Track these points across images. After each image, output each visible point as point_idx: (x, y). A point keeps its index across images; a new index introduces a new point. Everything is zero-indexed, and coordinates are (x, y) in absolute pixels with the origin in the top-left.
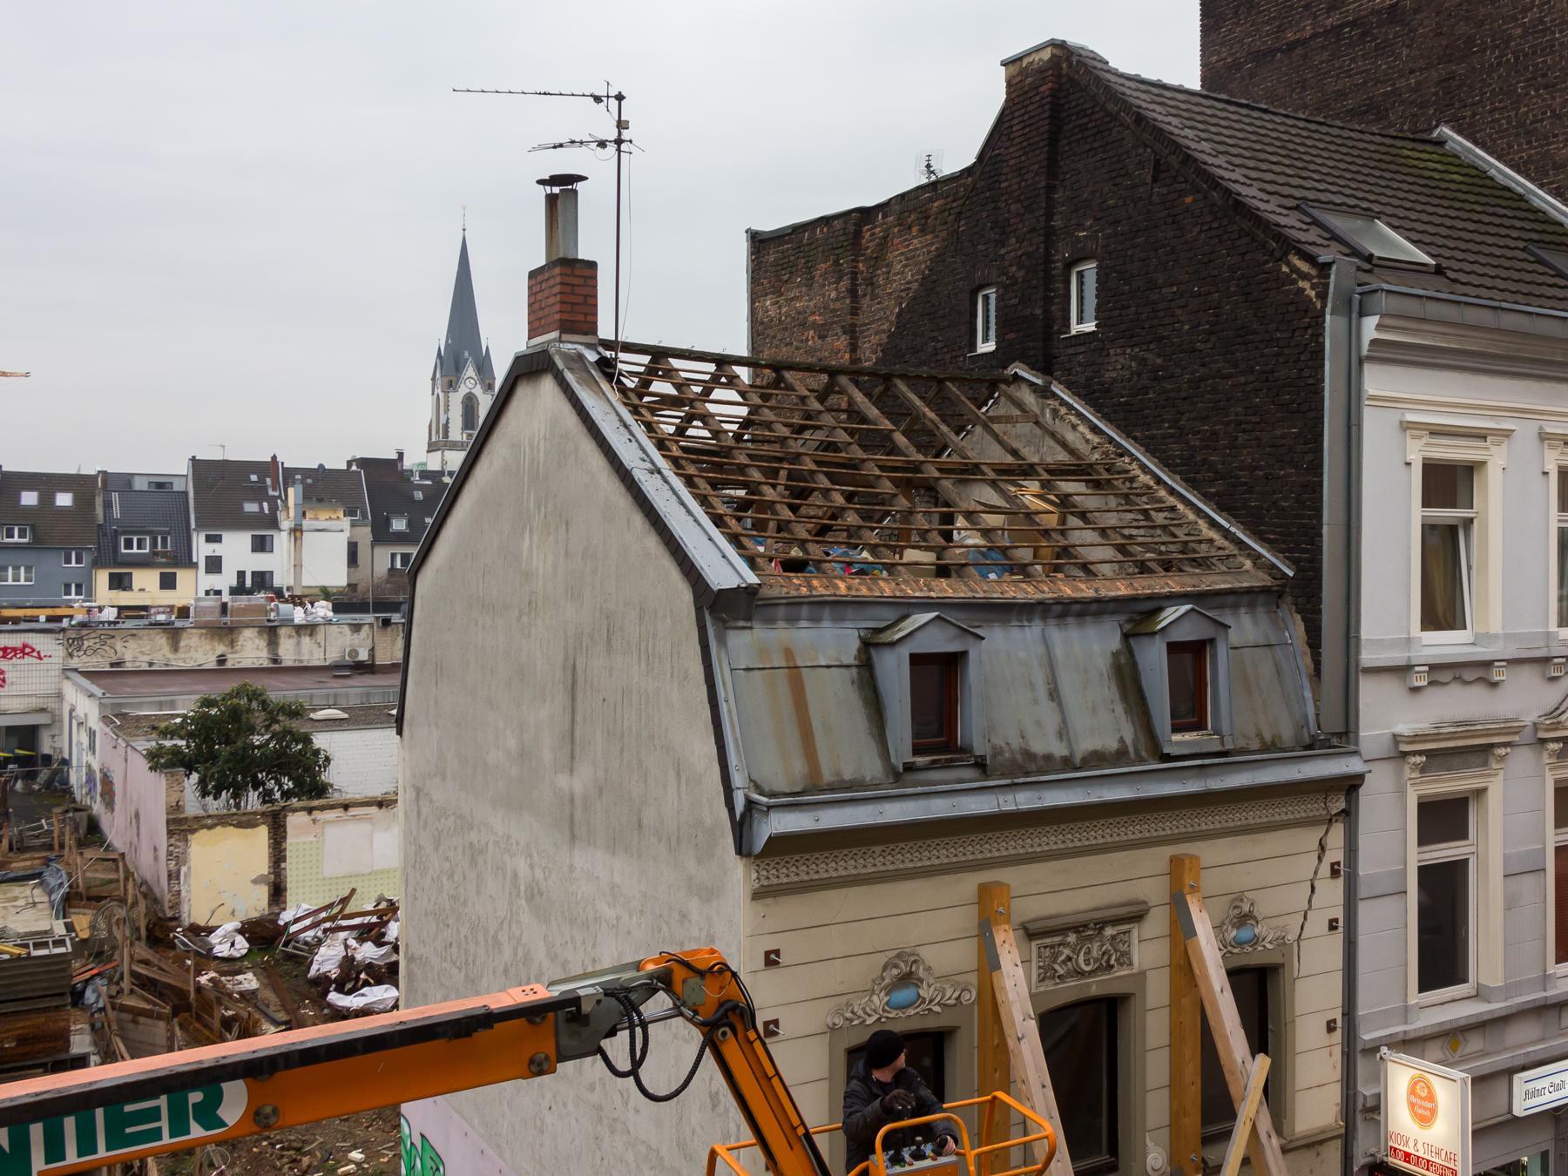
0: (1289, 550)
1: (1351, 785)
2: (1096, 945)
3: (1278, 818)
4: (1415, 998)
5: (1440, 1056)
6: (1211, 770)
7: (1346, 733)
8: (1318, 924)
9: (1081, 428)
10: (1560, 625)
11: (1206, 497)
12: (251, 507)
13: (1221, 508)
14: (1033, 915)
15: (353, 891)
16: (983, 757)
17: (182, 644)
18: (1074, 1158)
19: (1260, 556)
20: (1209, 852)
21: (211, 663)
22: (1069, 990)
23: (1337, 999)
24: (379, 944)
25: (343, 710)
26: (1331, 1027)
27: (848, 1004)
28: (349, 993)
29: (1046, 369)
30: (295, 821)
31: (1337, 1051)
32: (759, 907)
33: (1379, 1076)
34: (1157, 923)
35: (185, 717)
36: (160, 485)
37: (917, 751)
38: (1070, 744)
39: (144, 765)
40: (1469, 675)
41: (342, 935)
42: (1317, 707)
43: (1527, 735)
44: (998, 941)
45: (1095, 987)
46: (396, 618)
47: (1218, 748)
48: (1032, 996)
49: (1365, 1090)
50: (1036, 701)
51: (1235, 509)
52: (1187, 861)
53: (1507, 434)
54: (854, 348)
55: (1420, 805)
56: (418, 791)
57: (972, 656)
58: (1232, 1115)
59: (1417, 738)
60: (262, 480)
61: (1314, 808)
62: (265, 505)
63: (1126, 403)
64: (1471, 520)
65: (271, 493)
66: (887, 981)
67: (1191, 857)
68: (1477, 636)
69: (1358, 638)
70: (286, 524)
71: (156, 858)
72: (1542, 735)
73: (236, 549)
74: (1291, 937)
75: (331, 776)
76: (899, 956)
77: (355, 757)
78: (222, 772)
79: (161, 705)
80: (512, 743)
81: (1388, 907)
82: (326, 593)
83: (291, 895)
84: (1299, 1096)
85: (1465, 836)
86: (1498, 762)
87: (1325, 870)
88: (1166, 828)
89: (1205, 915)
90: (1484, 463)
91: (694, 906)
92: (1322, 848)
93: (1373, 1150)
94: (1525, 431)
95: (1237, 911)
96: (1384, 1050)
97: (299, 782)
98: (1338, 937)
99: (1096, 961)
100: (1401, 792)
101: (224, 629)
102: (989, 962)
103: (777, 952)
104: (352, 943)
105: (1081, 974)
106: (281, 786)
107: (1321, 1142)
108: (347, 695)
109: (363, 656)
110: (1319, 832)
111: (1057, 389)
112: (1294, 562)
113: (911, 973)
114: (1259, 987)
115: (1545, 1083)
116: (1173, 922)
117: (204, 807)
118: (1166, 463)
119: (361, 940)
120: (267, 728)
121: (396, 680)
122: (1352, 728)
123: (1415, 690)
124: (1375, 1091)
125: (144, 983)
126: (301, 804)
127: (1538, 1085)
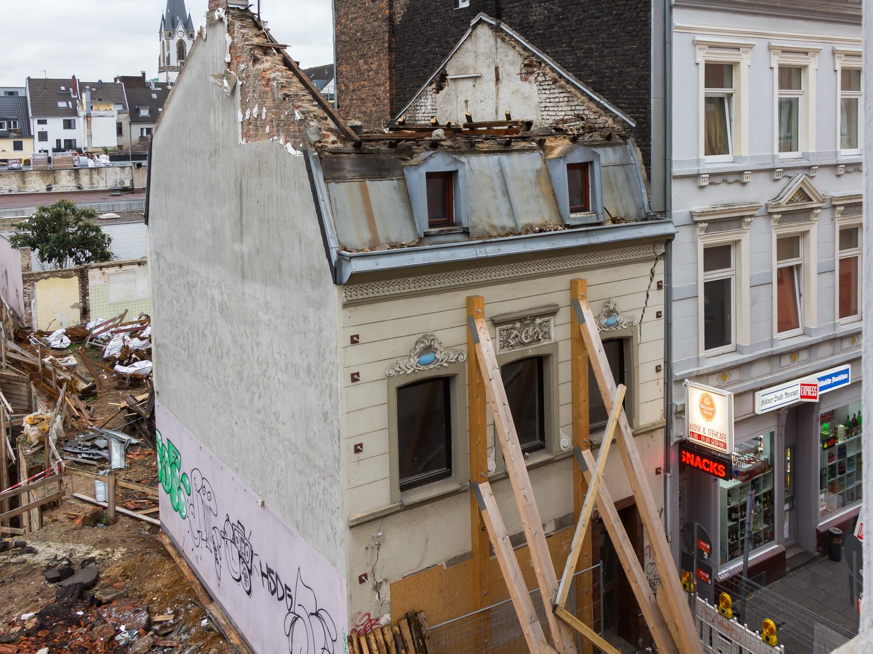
1: (667, 240)
3: (628, 258)
4: (703, 353)
5: (717, 384)
6: (591, 233)
7: (665, 212)
8: (651, 314)
9: (517, 48)
10: (780, 151)
11: (587, 84)
12: (62, 104)
13: (595, 90)
14: (496, 313)
15: (127, 311)
16: (467, 228)
17: (26, 180)
18: (521, 443)
19: (617, 116)
20: (590, 277)
21: (43, 189)
22: (517, 353)
23: (661, 354)
24: (142, 339)
25: (117, 213)
26: (658, 369)
27: (397, 363)
28: (126, 365)
29: (497, 14)
30: (94, 276)
31: (662, 382)
32: (347, 311)
33: (684, 395)
34: (564, 316)
35: (31, 218)
36: (11, 93)
37: (431, 225)
38: (515, 221)
39: (9, 245)
40: (731, 179)
41: (122, 334)
42: (649, 198)
43: (762, 211)
44: (478, 326)
45: (531, 351)
46: (145, 163)
47: (595, 221)
48: (497, 356)
49: (677, 402)
50: (495, 197)
52: (580, 284)
53: (751, 47)
54: (391, 7)
55: (705, 250)
56: (158, 254)
57: (460, 173)
58: (606, 417)
59: (703, 214)
60: (67, 90)
61: (648, 253)
62: (70, 103)
63: (541, 34)
64: (732, 94)
65: (73, 96)
66: (418, 350)
67: (582, 280)
68: (735, 157)
69: (671, 160)
70: (82, 113)
72: (770, 210)
73: (55, 128)
74: (636, 322)
75: (111, 249)
76: (424, 337)
77: (125, 239)
78: (52, 249)
79: (16, 213)
80: (208, 227)
81: (688, 305)
82: (106, 151)
84: (641, 406)
85: (729, 266)
86: (747, 226)
87: (654, 285)
89: (589, 311)
90: (738, 63)
91: (311, 312)
92: (653, 274)
93: (681, 434)
94: (761, 45)
96: (687, 380)
97: (94, 253)
98: (662, 321)
100: (695, 243)
101: (49, 171)
102: (473, 339)
103: (357, 336)
104: (127, 337)
105: (523, 344)
106: (85, 255)
107: (653, 430)
108: (119, 205)
109: (127, 184)
110: (651, 265)
111: (504, 27)
112: (636, 119)
113: (431, 345)
114: (619, 350)
115: (772, 396)
116: (572, 316)
117: (43, 268)
118: (565, 67)
119: (132, 337)
120: (76, 223)
121: (143, 197)
122: (668, 209)
123: (702, 187)
124: (682, 403)
125: (16, 363)
126: (96, 264)
127: (769, 397)
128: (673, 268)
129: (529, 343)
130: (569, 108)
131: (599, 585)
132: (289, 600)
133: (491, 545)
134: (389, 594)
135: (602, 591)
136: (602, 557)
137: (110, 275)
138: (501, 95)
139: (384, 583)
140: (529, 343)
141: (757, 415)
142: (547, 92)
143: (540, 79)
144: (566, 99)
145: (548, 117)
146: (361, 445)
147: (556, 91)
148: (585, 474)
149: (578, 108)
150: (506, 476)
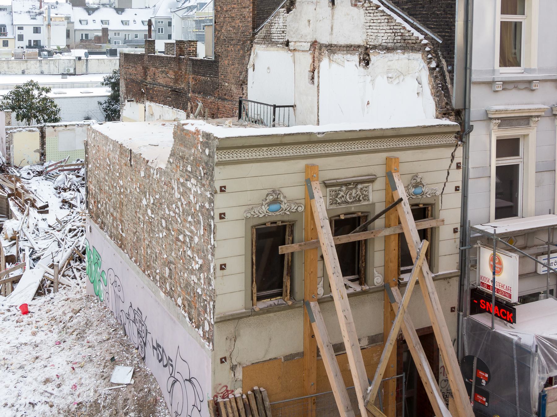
0: (438, 32)
2: (354, 191)
11: (403, 10)
13: (410, 15)
14: (327, 178)
20: (403, 156)
27: (252, 209)
34: (380, 184)
44: (313, 188)
45: (353, 208)
48: (327, 210)
51: (415, 14)
52: (393, 160)
66: (268, 201)
69: (471, 70)
71: (2, 142)
83: (47, 157)
88: (385, 144)
95: (415, 181)
99: (354, 198)
103: (225, 187)
105: (347, 203)
112: (442, 37)
128: (470, 153)
129: (352, 202)
130: (389, 28)
131: (401, 391)
132: (171, 368)
133: (318, 349)
134: (241, 374)
135: (404, 396)
136: (405, 370)
137: (59, 131)
139: (238, 366)
140: (352, 202)
142: (372, 15)
143: (366, 5)
144: (386, 21)
145: (372, 34)
146: (225, 265)
147: (378, 14)
148: (393, 304)
149: (395, 27)
150: (331, 299)
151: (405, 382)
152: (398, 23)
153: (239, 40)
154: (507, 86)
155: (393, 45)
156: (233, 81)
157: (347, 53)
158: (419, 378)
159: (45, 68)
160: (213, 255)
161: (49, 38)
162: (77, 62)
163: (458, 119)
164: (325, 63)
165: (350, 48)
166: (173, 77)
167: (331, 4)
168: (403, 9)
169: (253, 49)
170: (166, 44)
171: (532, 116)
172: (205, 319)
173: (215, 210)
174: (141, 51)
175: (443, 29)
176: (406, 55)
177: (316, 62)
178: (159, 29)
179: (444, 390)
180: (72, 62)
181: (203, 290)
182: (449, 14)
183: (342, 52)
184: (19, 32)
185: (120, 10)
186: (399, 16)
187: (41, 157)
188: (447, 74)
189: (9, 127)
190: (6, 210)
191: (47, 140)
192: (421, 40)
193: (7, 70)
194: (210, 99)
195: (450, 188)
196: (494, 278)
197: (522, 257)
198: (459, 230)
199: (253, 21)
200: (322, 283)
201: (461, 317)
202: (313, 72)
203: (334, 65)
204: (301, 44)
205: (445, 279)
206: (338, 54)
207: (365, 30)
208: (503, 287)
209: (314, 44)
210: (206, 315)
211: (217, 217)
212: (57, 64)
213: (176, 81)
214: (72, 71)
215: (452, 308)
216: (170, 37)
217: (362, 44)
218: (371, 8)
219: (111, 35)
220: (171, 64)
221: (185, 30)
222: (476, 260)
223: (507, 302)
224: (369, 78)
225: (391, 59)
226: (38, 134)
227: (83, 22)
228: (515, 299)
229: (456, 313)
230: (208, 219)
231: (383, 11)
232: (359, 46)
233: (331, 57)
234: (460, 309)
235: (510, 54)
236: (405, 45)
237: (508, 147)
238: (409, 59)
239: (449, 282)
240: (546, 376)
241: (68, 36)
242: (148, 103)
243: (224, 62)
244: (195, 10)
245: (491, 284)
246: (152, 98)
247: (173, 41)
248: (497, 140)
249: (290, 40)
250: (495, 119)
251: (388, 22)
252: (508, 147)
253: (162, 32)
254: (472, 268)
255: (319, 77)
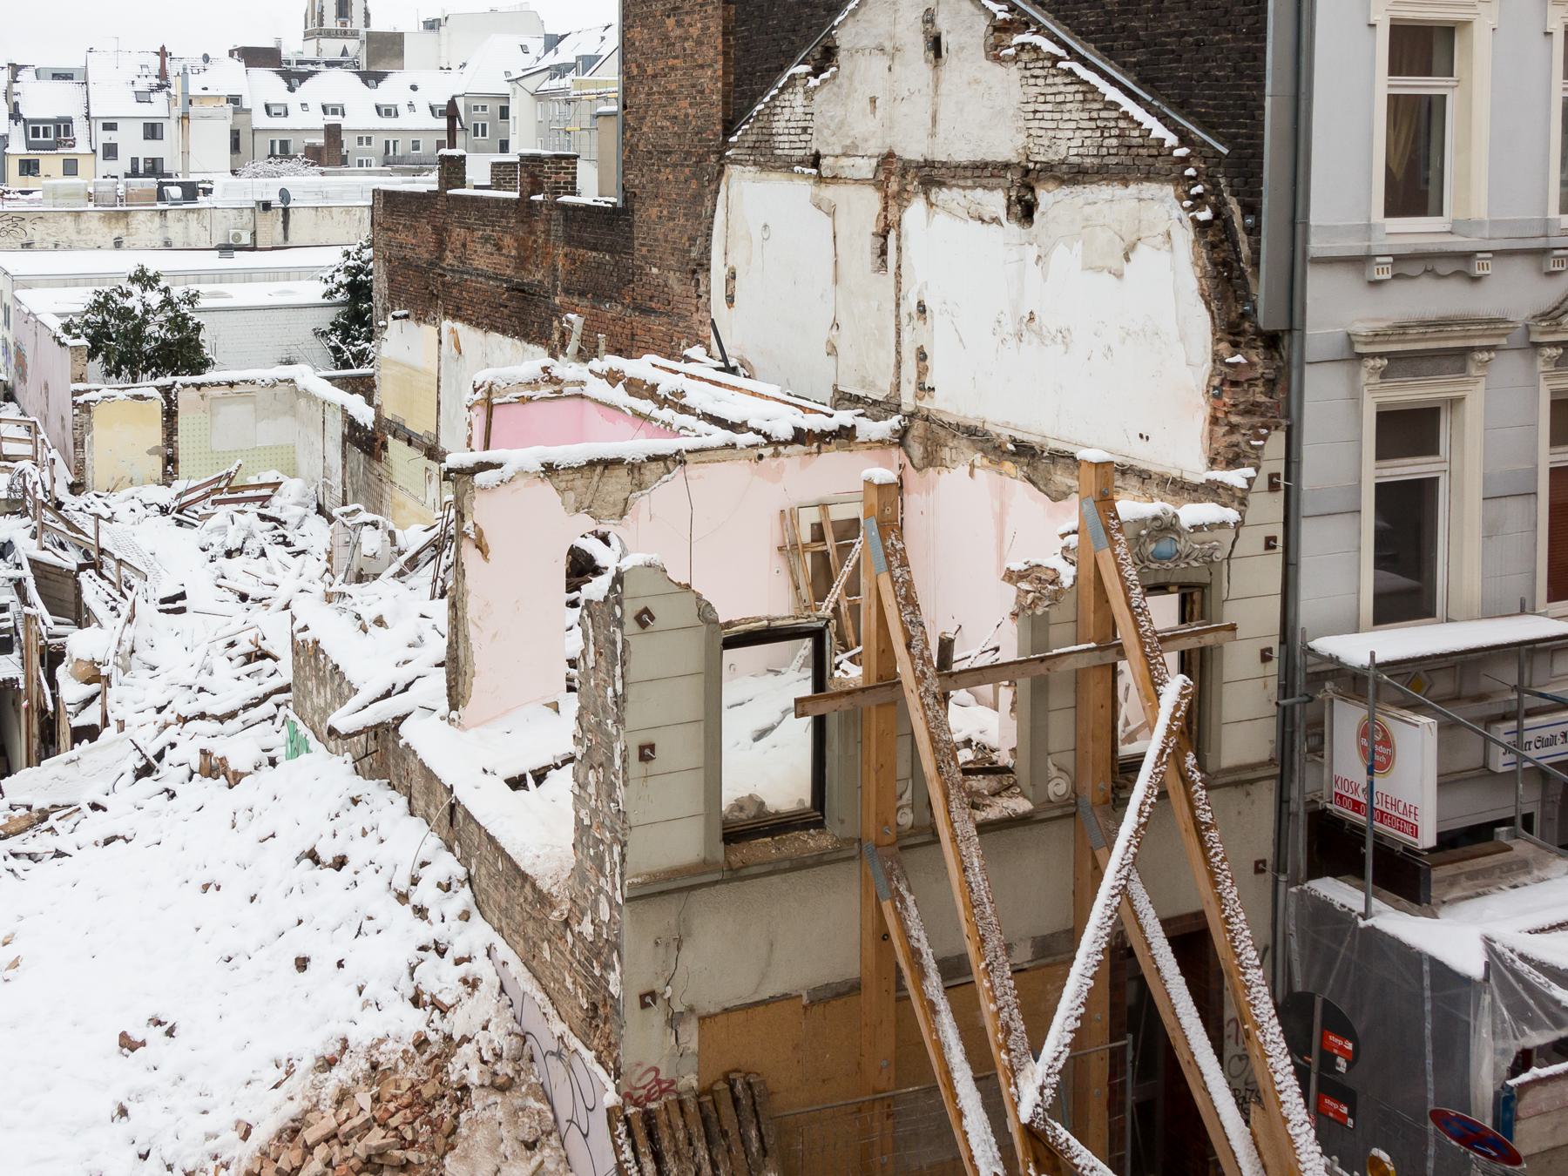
11: (1125, 67)
13: (1141, 82)
19: (1188, 132)
51: (1158, 79)
130: (1086, 115)
135: (1130, 1099)
136: (1134, 1029)
138: (943, 88)
141: (1494, 773)
142: (1041, 82)
144: (1080, 97)
147: (1058, 80)
149: (1104, 114)
151: (1133, 1062)
152: (1112, 103)
153: (688, 153)
154: (1405, 269)
155: (1096, 161)
156: (672, 262)
157: (973, 188)
158: (1170, 1050)
159: (175, 231)
160: (619, 721)
161: (186, 153)
162: (260, 215)
163: (1272, 358)
164: (915, 212)
165: (982, 172)
166: (514, 253)
167: (931, 55)
168: (1124, 65)
169: (724, 179)
170: (495, 165)
171: (1472, 349)
172: (600, 890)
173: (626, 603)
174: (428, 182)
175: (1233, 117)
176: (1133, 188)
177: (893, 209)
178: (476, 126)
179: (1239, 1084)
180: (247, 214)
181: (594, 812)
182: (1249, 76)
183: (961, 183)
184: (105, 137)
185: (372, 78)
186: (1113, 82)
187: (165, 467)
188: (1242, 236)
189: (81, 386)
190: (73, 607)
191: (182, 421)
192: (1172, 148)
193: (74, 237)
194: (611, 310)
195: (1251, 541)
196: (1371, 784)
197: (1447, 728)
198: (1276, 653)
199: (726, 103)
200: (908, 795)
201: (1282, 887)
202: (884, 235)
203: (941, 218)
204: (850, 161)
205: (1237, 784)
206: (950, 187)
207: (1021, 123)
208: (1395, 805)
209: (887, 159)
210: (602, 880)
211: (631, 625)
212: (207, 223)
213: (522, 262)
214: (246, 239)
215: (1257, 863)
216: (504, 147)
217: (1015, 160)
218: (1040, 64)
219: (349, 142)
220: (506, 217)
221: (545, 129)
222: (1322, 736)
223: (1406, 849)
224: (1033, 252)
225: (1091, 198)
226: (159, 401)
227: (274, 110)
228: (1427, 839)
229: (1269, 875)
230: (607, 627)
231: (1070, 72)
232: (1007, 166)
233: (933, 198)
234: (1280, 867)
235: (1413, 184)
236: (1129, 162)
237: (1408, 430)
238: (1140, 200)
239: (1248, 794)
240: (1515, 1046)
241: (235, 146)
242: (447, 324)
243: (648, 212)
244: (571, 76)
245: (1362, 798)
246: (459, 309)
247: (512, 157)
248: (1379, 414)
249: (822, 152)
250: (1373, 356)
251: (1084, 101)
252: (1408, 430)
253: (484, 134)
254: (1309, 757)
255: (899, 249)
